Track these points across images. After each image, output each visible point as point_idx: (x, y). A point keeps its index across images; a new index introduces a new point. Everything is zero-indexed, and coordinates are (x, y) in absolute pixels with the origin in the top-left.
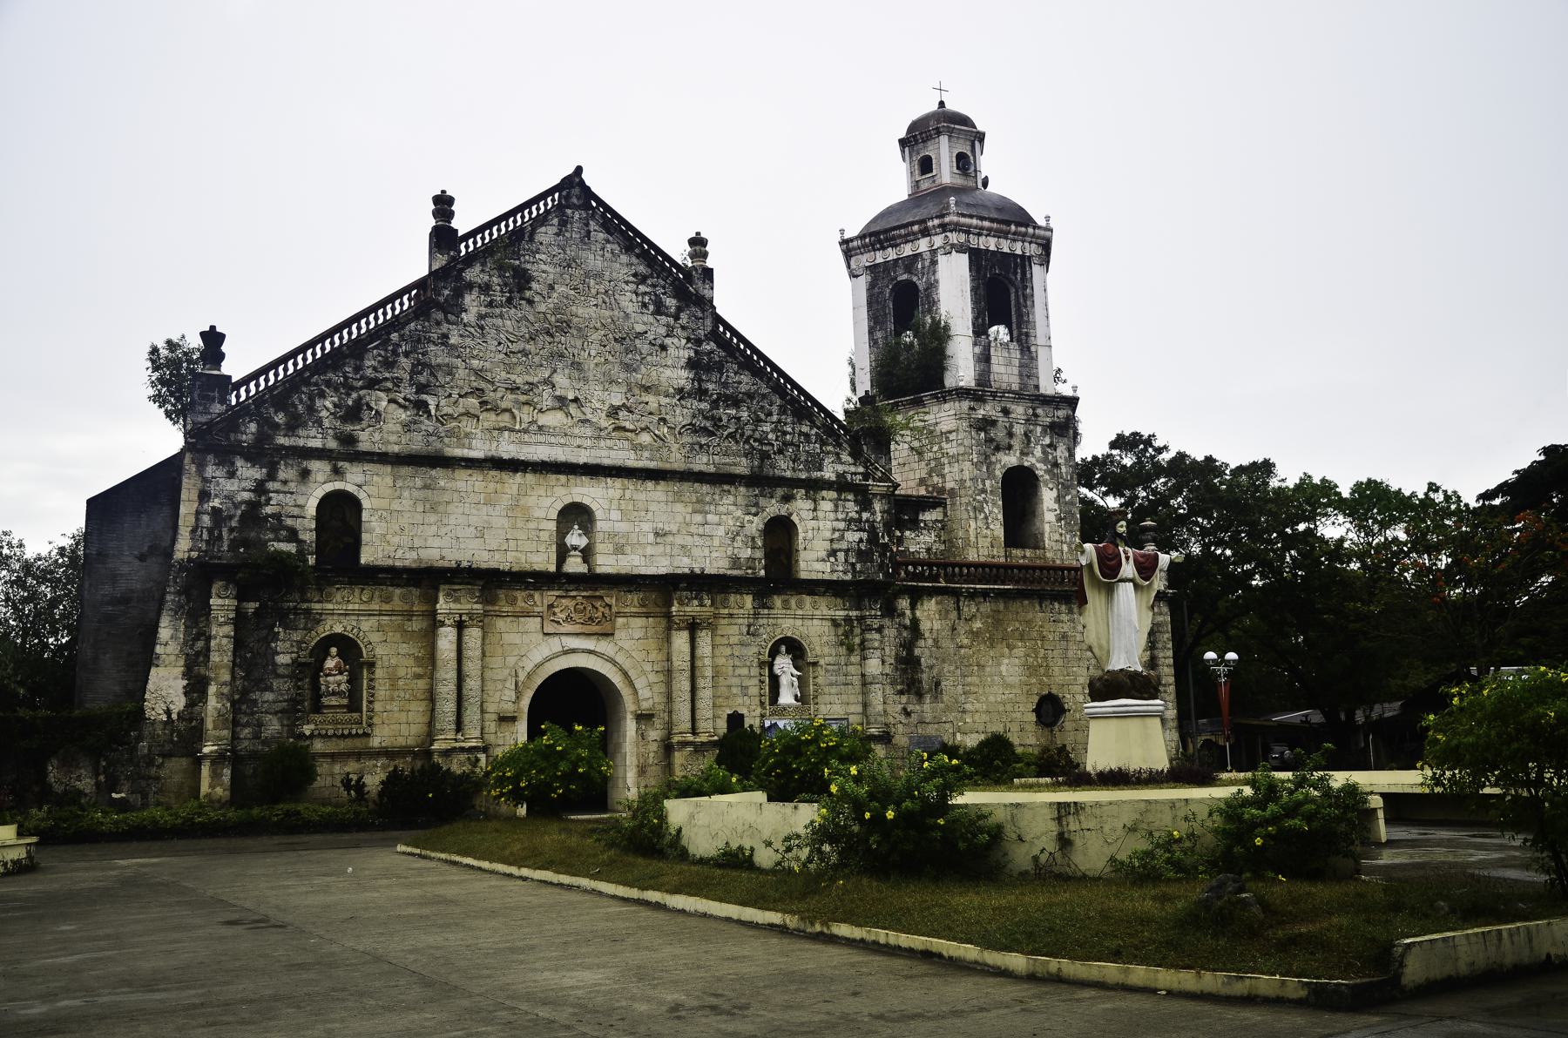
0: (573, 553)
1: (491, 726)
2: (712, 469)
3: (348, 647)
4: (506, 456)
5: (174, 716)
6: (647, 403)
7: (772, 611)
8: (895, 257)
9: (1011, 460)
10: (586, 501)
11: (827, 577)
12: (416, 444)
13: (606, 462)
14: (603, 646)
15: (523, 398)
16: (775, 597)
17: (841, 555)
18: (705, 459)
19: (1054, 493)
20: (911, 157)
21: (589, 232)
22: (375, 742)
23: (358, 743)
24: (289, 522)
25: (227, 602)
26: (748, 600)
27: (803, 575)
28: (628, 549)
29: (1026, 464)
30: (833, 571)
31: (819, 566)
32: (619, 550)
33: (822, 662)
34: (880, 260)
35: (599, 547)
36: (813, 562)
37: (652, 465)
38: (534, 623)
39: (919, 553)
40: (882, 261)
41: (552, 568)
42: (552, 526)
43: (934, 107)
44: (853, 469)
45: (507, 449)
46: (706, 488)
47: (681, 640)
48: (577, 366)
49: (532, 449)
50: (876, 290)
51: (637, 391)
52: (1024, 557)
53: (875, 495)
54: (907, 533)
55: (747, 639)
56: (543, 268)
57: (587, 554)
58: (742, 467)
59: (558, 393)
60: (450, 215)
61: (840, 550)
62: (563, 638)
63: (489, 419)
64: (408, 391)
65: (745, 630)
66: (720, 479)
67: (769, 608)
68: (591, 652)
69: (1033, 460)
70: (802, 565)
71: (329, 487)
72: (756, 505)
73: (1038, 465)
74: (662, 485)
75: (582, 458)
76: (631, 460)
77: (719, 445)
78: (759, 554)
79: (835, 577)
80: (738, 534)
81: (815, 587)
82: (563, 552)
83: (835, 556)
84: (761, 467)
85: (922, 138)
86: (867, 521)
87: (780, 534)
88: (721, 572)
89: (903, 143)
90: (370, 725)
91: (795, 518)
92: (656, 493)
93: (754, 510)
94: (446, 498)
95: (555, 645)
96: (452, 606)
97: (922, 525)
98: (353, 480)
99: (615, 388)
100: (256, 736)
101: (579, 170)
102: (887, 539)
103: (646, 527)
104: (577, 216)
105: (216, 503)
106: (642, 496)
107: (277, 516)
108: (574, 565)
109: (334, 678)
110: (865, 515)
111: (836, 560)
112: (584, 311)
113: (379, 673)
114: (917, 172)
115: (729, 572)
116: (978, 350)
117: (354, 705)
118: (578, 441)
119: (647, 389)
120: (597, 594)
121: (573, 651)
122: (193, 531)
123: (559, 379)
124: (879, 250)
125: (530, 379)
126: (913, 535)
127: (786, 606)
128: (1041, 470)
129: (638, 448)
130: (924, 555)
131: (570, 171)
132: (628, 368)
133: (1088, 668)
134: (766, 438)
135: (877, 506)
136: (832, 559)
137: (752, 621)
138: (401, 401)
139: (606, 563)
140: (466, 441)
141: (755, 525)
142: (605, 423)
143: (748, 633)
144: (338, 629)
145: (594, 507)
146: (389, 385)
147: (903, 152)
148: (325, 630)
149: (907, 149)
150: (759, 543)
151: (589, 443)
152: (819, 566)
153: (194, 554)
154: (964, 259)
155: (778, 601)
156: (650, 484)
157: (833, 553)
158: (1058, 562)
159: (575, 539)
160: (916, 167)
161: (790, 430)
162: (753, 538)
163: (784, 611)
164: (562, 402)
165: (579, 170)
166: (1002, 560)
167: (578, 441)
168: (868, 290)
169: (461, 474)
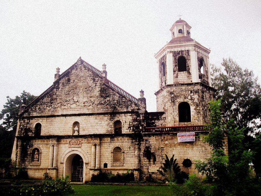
0: (76, 131)
1: (59, 164)
2: (103, 112)
3: (37, 150)
4: (64, 114)
5: (14, 162)
6: (91, 100)
7: (114, 141)
9: (180, 100)
11: (128, 133)
12: (50, 113)
13: (82, 113)
14: (79, 149)
15: (68, 102)
16: (115, 138)
17: (132, 128)
18: (102, 110)
19: (194, 107)
21: (81, 69)
22: (41, 167)
23: (37, 167)
24: (31, 129)
25: (20, 143)
26: (109, 139)
27: (123, 133)
28: (85, 130)
29: (185, 101)
30: (129, 132)
31: (126, 131)
32: (84, 130)
33: (125, 152)
35: (80, 130)
36: (125, 130)
37: (91, 112)
38: (67, 145)
39: (159, 125)
41: (71, 135)
42: (72, 126)
43: (179, 19)
44: (135, 108)
45: (65, 113)
46: (102, 116)
47: (93, 147)
48: (78, 95)
49: (69, 112)
51: (89, 98)
52: (184, 124)
53: (141, 113)
54: (156, 121)
55: (108, 147)
56: (73, 77)
57: (78, 132)
58: (110, 110)
59: (74, 101)
60: (59, 72)
61: (132, 127)
62: (72, 148)
63: (63, 107)
64: (49, 104)
65: (108, 145)
66: (104, 114)
67: (113, 141)
68: (76, 150)
69: (188, 100)
70: (122, 131)
72: (112, 118)
73: (189, 101)
74: (93, 116)
75: (77, 113)
76: (87, 112)
77: (105, 107)
78: (113, 129)
79: (130, 133)
80: (108, 125)
81: (124, 135)
82: (74, 131)
83: (130, 128)
84: (114, 110)
86: (139, 119)
87: (118, 124)
88: (104, 133)
90: (40, 164)
91: (121, 121)
92: (92, 118)
93: (112, 119)
94: (54, 122)
95: (70, 149)
96: (52, 142)
97: (160, 119)
98: (40, 121)
99: (85, 98)
100: (25, 165)
101: (80, 58)
102: (143, 123)
103: (89, 125)
104: (79, 66)
105: (22, 127)
106: (88, 119)
107: (29, 128)
108: (76, 134)
109: (36, 156)
110: (138, 118)
111: (131, 129)
112: (80, 84)
113: (42, 155)
115: (106, 133)
116: (175, 75)
117: (38, 161)
118: (77, 109)
119: (91, 97)
120: (78, 139)
121: (74, 150)
122: (18, 131)
123: (75, 98)
125: (69, 99)
126: (158, 121)
127: (118, 140)
128: (190, 102)
129: (88, 109)
130: (160, 126)
132: (87, 93)
133: (200, 152)
134: (115, 104)
135: (141, 116)
136: (130, 129)
137: (110, 143)
138: (48, 106)
139: (82, 133)
140: (58, 112)
141: (112, 123)
142: (83, 105)
143: (109, 146)
144: (36, 147)
146: (47, 104)
148: (34, 147)
150: (113, 126)
151: (79, 109)
152: (126, 131)
153: (18, 135)
154: (172, 54)
155: (116, 139)
156: (90, 116)
157: (130, 127)
158: (195, 125)
159: (76, 128)
161: (121, 101)
162: (111, 126)
163: (117, 141)
164: (75, 102)
165: (80, 58)
166: (178, 126)
167: (77, 109)
169: (57, 118)
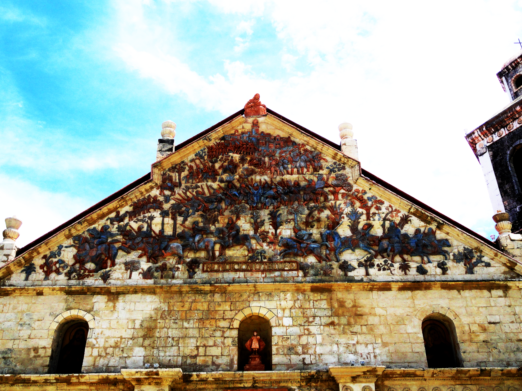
8: (507, 132)
10: (263, 312)
20: (507, 81)
34: (496, 138)
40: (498, 138)
50: (498, 158)
71: (67, 314)
85: (512, 67)
89: (500, 75)
101: (257, 97)
114: (514, 87)
124: (494, 133)
131: (252, 97)
145: (268, 316)
147: (502, 82)
149: (504, 78)
160: (513, 85)
165: (257, 97)
168: (492, 161)
